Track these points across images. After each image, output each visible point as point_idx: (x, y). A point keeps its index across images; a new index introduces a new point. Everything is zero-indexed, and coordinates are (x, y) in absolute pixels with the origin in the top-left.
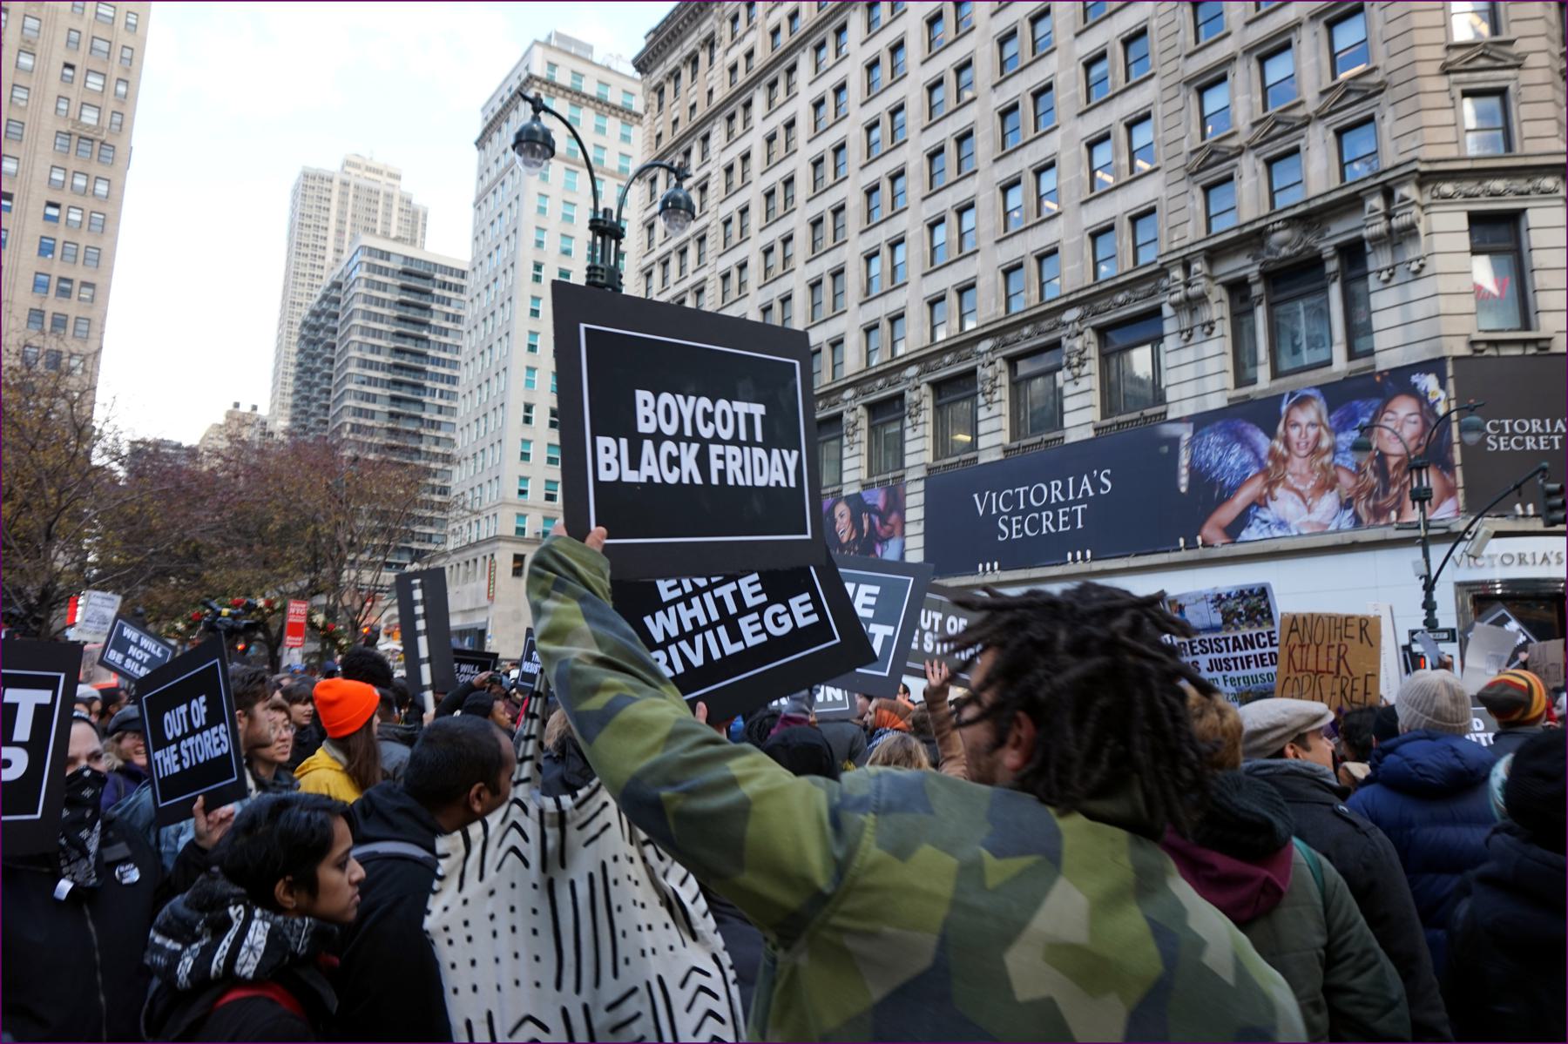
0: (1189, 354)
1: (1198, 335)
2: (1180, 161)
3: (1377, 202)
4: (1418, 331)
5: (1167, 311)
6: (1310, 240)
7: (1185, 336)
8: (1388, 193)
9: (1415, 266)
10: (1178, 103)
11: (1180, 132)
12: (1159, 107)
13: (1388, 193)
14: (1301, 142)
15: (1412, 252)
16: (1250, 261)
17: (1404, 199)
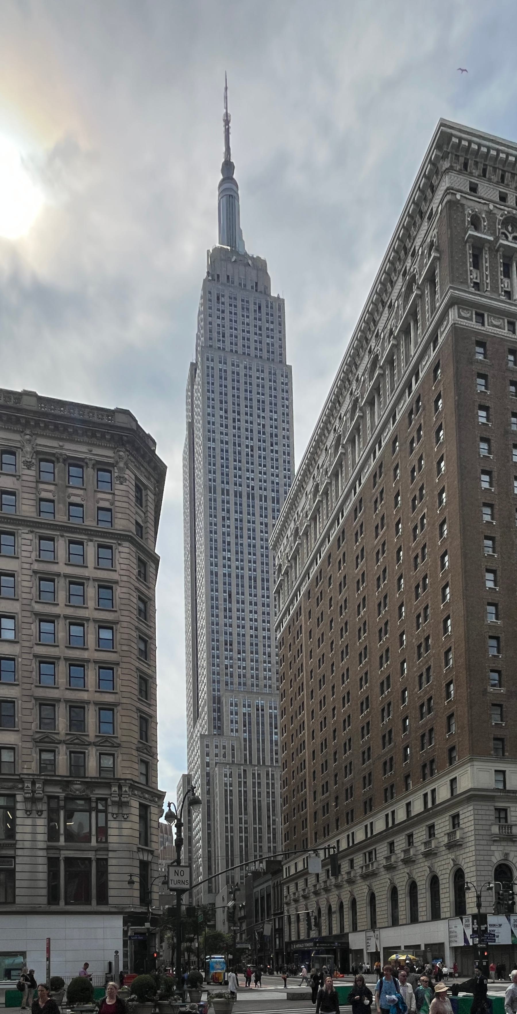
0: (29, 821)
1: (34, 814)
2: (30, 733)
3: (115, 789)
4: (124, 840)
5: (19, 798)
6: (88, 792)
7: (28, 813)
8: (120, 788)
9: (125, 817)
10: (30, 705)
11: (30, 719)
12: (20, 702)
13: (120, 788)
14: (86, 751)
15: (125, 811)
16: (61, 791)
17: (126, 791)
